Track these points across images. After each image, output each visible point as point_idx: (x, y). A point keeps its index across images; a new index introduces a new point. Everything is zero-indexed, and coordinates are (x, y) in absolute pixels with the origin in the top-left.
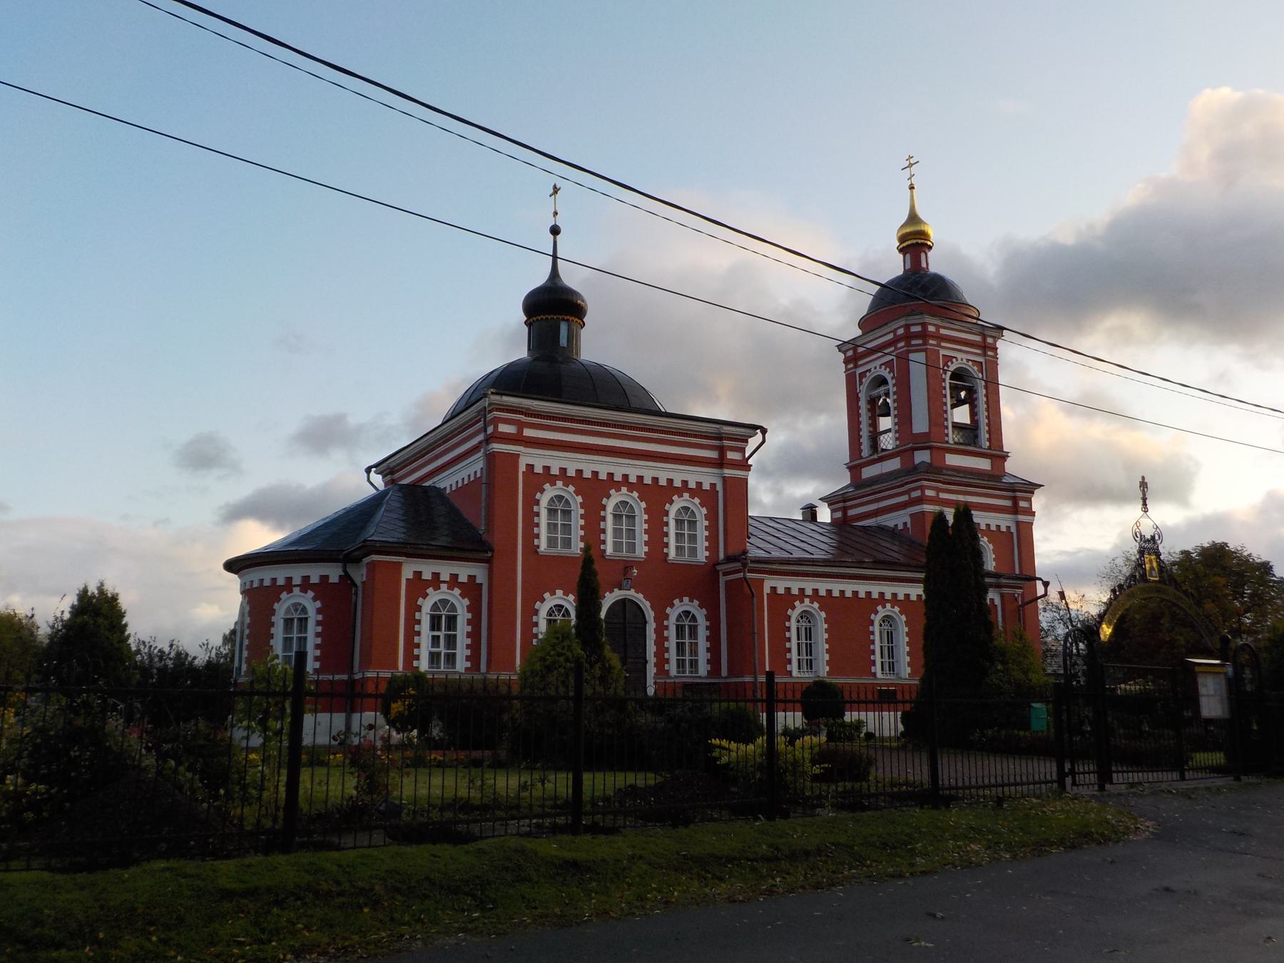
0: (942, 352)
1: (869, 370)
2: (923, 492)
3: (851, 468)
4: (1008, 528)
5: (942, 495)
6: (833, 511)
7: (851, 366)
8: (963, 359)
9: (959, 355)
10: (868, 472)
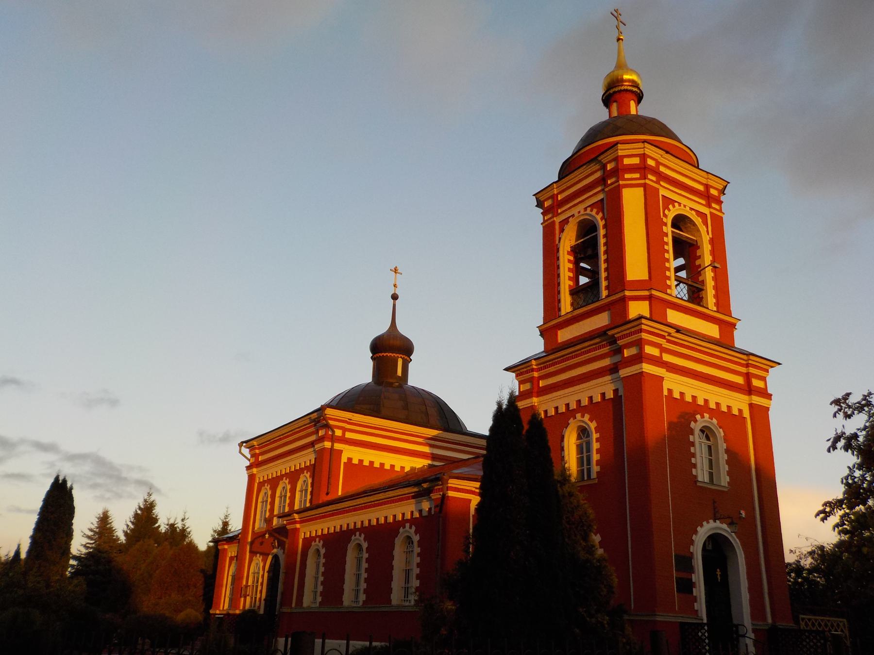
0: (662, 192)
1: (573, 216)
2: (641, 349)
3: (543, 332)
4: (740, 411)
5: (667, 357)
6: (521, 383)
7: (550, 216)
8: (687, 205)
9: (683, 201)
10: (564, 335)
